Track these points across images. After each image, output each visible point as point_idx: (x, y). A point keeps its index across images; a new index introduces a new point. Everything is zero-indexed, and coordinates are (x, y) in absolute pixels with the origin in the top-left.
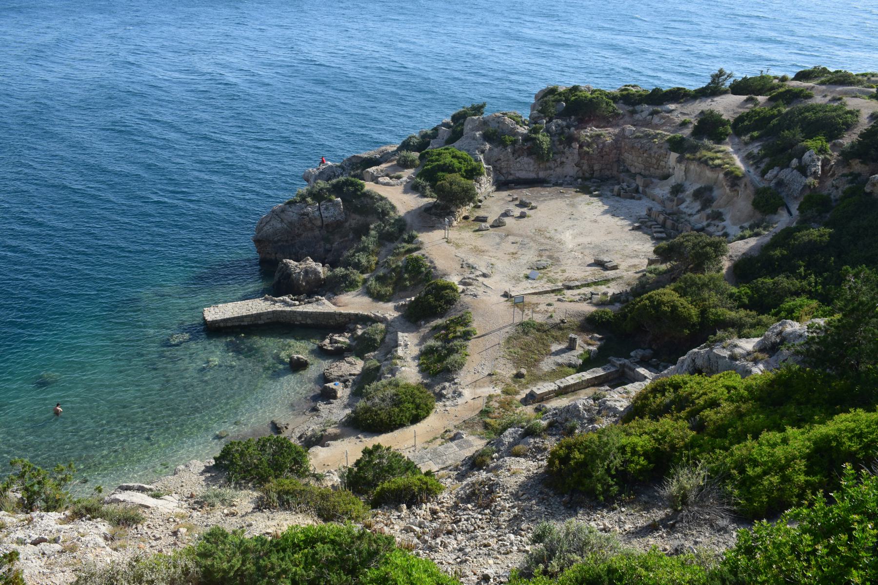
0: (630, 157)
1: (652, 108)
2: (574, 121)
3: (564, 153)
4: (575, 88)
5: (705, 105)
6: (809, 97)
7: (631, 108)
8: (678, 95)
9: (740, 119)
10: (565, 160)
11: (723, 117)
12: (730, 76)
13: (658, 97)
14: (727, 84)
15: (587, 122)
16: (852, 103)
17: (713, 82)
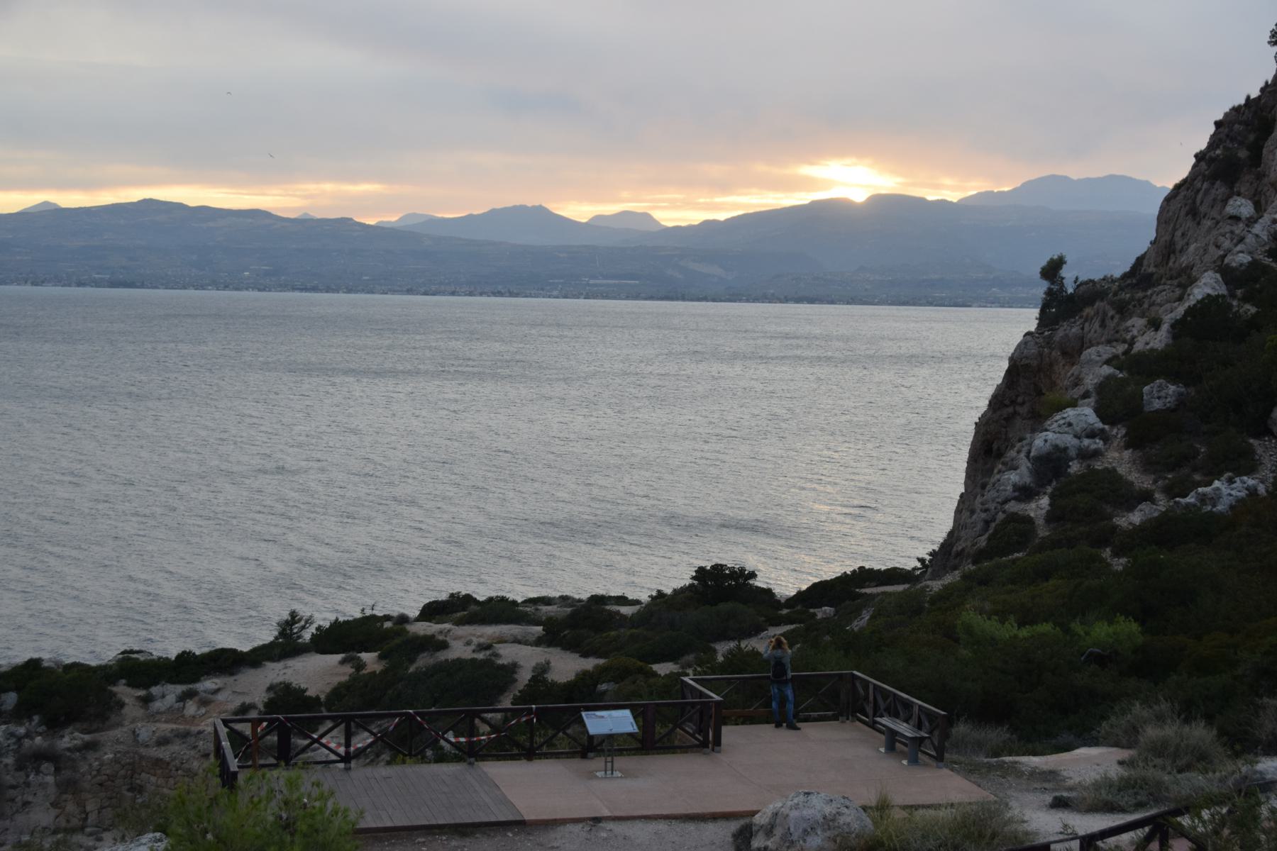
0: (153, 779)
1: (180, 689)
2: (40, 724)
3: (28, 785)
4: (34, 664)
5: (275, 672)
6: (444, 646)
7: (142, 693)
8: (225, 662)
9: (338, 693)
10: (30, 798)
11: (308, 694)
12: (309, 621)
13: (188, 668)
14: (307, 636)
15: (64, 725)
16: (508, 653)
17: (282, 634)
